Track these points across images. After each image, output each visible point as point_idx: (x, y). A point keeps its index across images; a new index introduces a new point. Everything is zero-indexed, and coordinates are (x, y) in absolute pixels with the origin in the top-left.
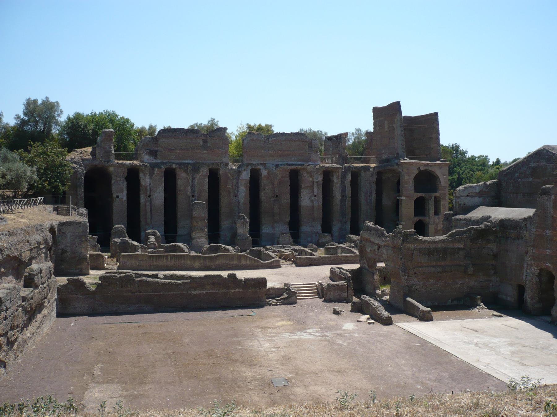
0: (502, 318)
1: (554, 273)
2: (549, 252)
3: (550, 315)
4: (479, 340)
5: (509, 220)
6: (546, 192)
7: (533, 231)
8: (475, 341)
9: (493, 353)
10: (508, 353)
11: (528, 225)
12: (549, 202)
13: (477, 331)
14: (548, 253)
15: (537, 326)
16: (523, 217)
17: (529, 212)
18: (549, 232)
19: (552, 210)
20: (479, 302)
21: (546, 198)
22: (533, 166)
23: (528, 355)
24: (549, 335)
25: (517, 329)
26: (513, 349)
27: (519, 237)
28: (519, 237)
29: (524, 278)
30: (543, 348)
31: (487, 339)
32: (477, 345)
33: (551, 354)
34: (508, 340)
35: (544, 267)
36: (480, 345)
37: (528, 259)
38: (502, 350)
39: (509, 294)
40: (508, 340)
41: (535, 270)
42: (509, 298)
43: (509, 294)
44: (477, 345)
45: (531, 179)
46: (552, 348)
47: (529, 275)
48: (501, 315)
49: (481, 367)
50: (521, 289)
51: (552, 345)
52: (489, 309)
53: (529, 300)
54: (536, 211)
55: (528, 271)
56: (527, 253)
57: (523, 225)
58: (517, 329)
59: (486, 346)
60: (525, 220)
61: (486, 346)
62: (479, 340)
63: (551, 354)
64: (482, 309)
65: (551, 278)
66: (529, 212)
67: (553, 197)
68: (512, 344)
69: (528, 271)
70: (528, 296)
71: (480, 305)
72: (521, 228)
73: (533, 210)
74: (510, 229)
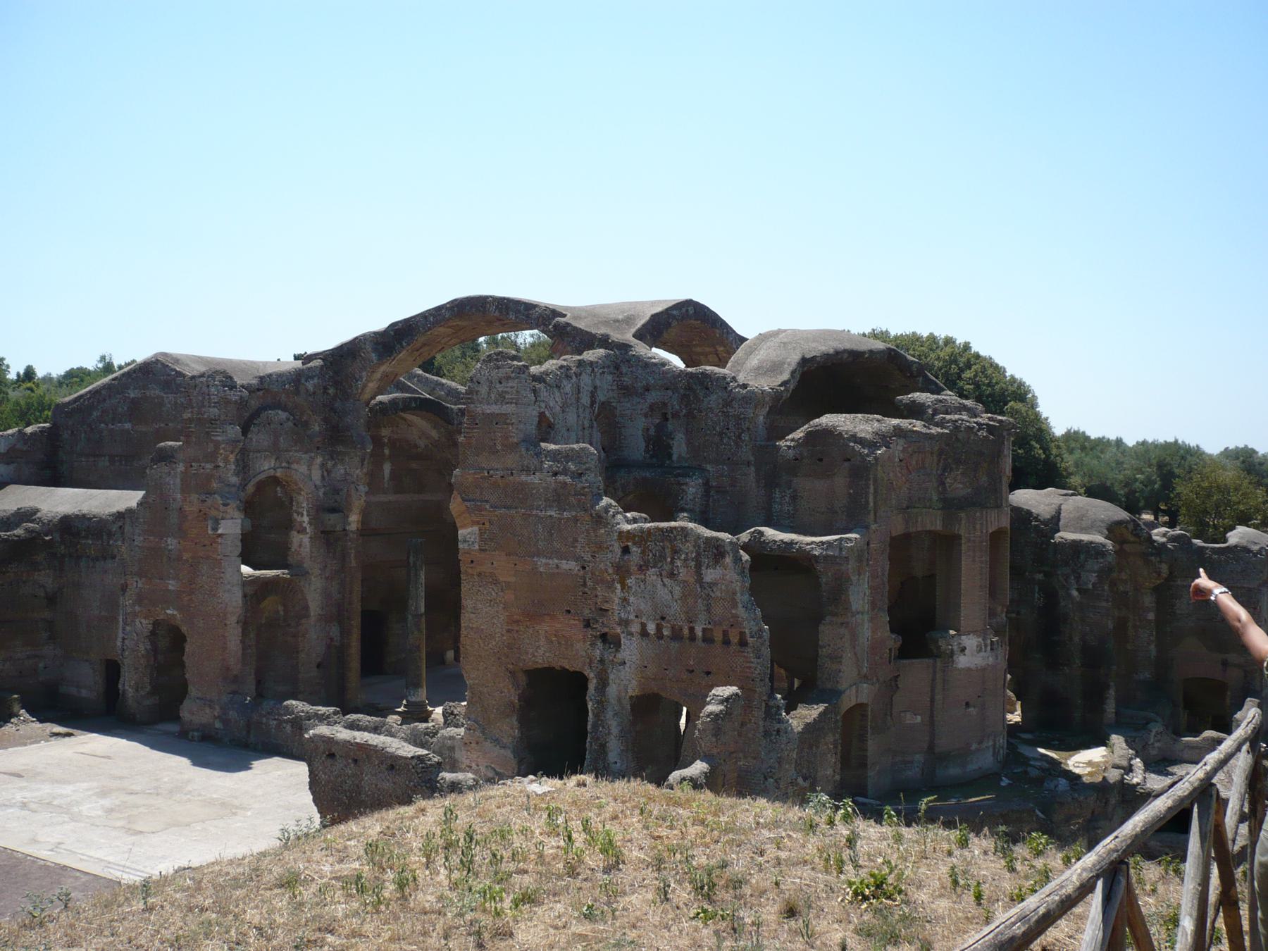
0: (72, 738)
1: (184, 629)
2: (172, 585)
3: (176, 718)
4: (28, 794)
5: (83, 518)
6: (166, 457)
7: (139, 540)
8: (19, 797)
9: (66, 818)
10: (100, 813)
11: (127, 528)
12: (173, 477)
13: (19, 776)
14: (170, 587)
15: (154, 746)
16: (114, 510)
17: (129, 499)
18: (172, 543)
19: (179, 496)
20: (16, 708)
21: (166, 469)
22: (132, 395)
23: (142, 810)
24: (184, 762)
25: (109, 758)
26: (107, 802)
27: (106, 555)
28: (106, 555)
29: (119, 644)
30: (171, 792)
31: (46, 789)
32: (24, 806)
33: (189, 800)
34: (95, 784)
35: (161, 617)
36: (33, 806)
37: (127, 601)
38: (85, 808)
39: (85, 682)
40: (95, 784)
41: (143, 625)
42: (84, 693)
43: (85, 682)
44: (24, 806)
45: (128, 426)
46: (189, 788)
47: (131, 639)
48: (70, 730)
49: (43, 853)
50: (112, 670)
51: (189, 781)
52: (41, 722)
53: (130, 692)
54: (144, 497)
55: (128, 628)
56: (124, 589)
57: (114, 528)
58: (109, 758)
59: (48, 805)
60: (120, 516)
61: (48, 805)
62: (28, 794)
63: (189, 800)
64: (25, 724)
65: (178, 639)
66: (129, 499)
67: (181, 467)
68: (104, 793)
69: (128, 628)
70: (130, 683)
71: (17, 716)
72: (110, 534)
73: (138, 495)
74: (86, 537)
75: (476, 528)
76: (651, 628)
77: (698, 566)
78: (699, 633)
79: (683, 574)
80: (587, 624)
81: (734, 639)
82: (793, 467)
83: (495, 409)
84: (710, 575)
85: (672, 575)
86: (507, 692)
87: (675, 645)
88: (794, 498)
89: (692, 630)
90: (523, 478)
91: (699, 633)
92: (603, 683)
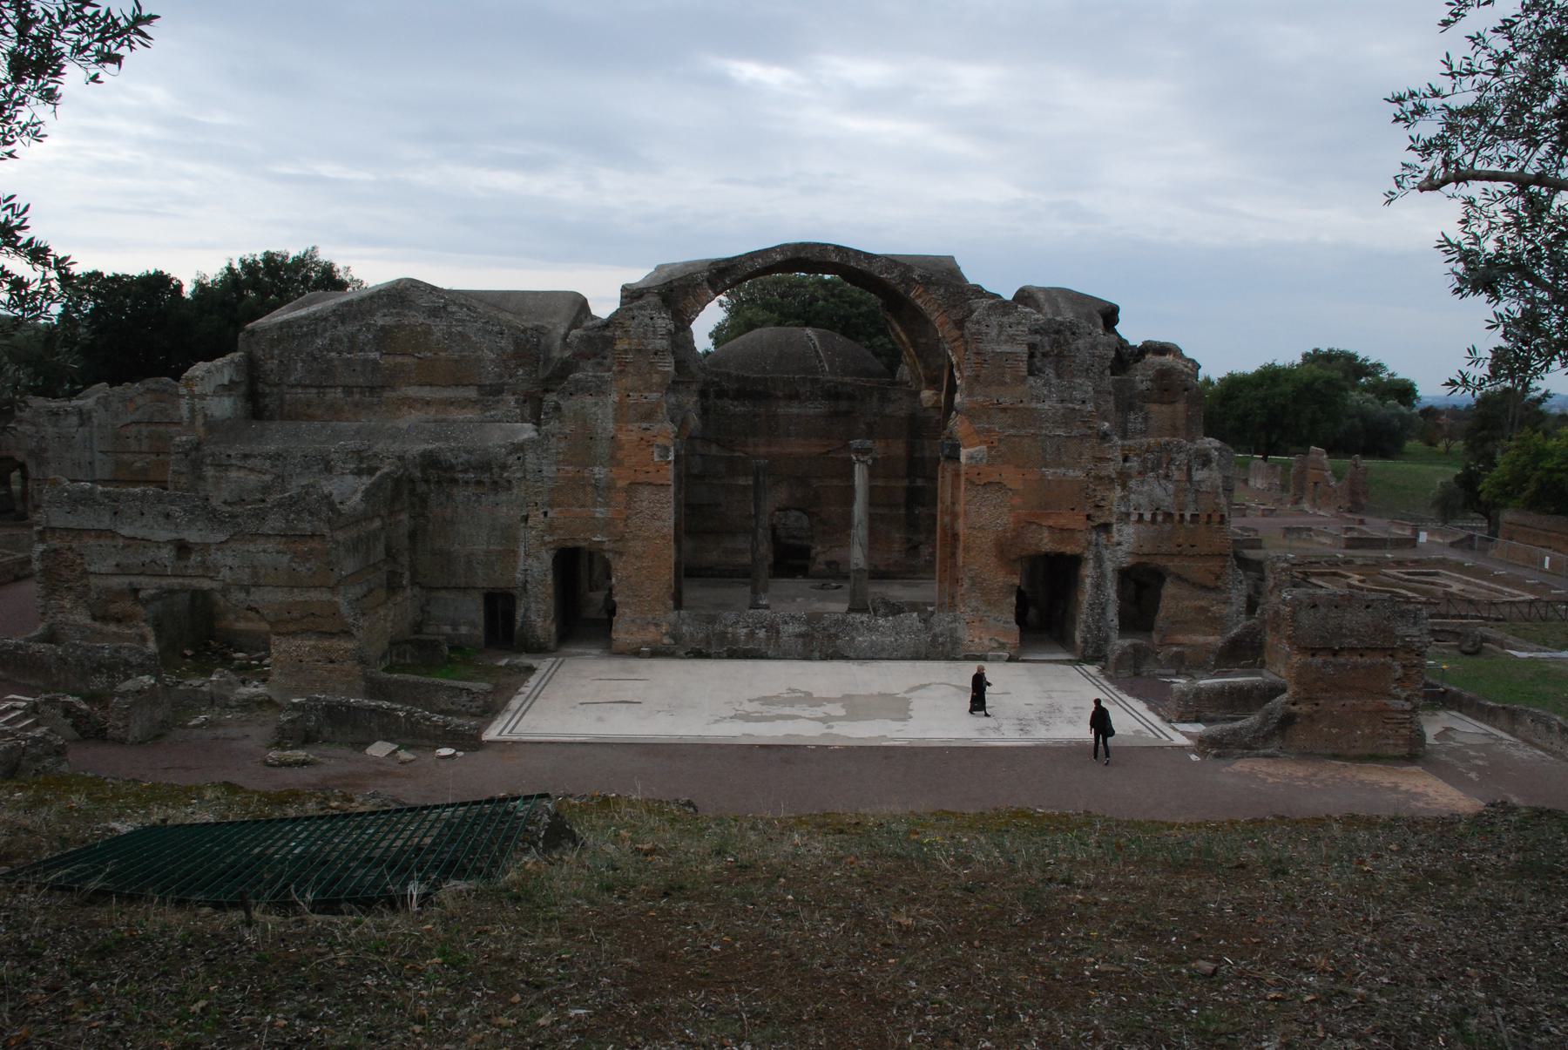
75: (984, 447)
76: (1148, 517)
77: (1189, 470)
78: (1188, 517)
79: (1176, 475)
80: (1088, 517)
81: (1216, 518)
82: (1146, 397)
83: (1006, 348)
84: (1198, 475)
85: (1167, 477)
86: (1006, 580)
87: (1168, 527)
88: (1146, 419)
89: (1182, 516)
90: (1033, 405)
91: (1188, 517)
92: (1099, 561)
